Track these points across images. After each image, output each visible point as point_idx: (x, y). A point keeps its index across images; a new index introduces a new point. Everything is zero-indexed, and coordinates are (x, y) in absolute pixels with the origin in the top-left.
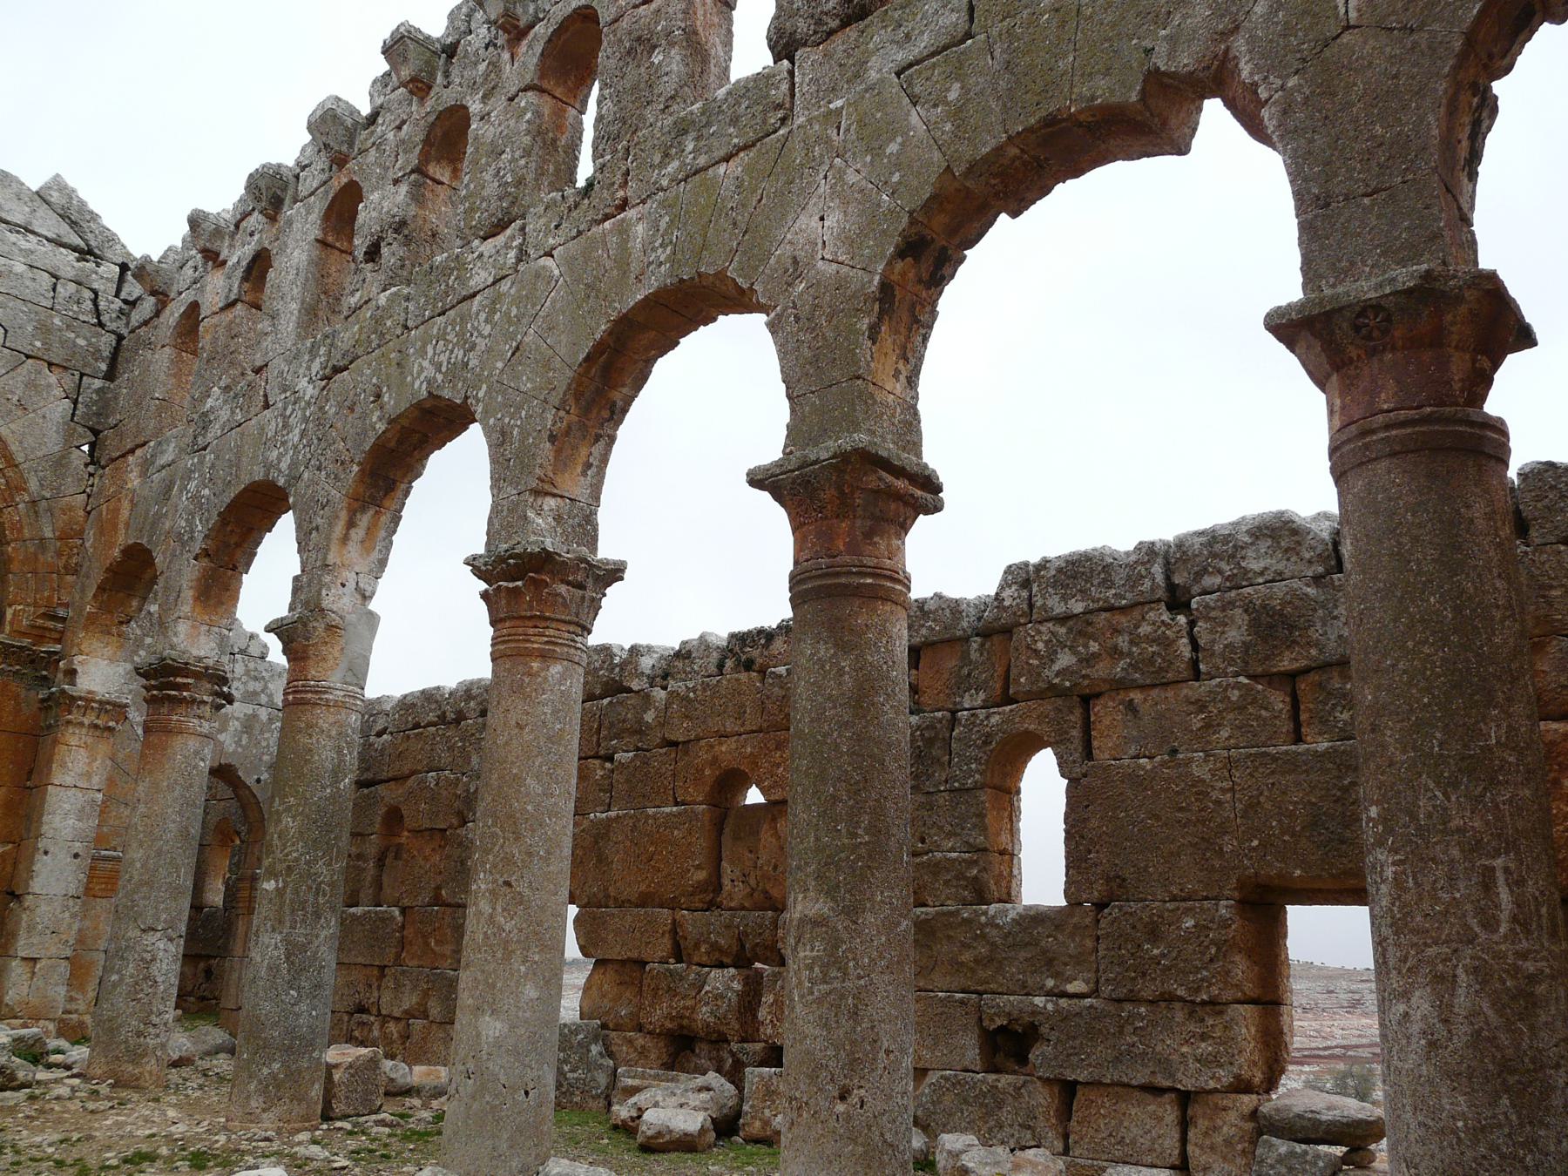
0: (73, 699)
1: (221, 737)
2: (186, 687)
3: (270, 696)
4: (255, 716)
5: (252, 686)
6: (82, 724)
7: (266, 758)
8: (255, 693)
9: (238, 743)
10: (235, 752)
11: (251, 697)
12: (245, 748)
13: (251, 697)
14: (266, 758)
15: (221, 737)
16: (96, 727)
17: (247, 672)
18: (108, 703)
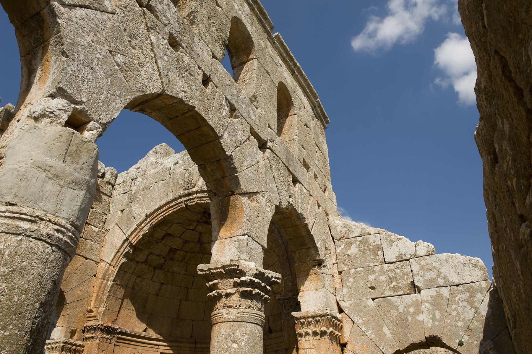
0: (297, 319)
1: (420, 318)
2: (214, 287)
3: (445, 278)
4: (439, 295)
5: (430, 275)
6: (307, 334)
7: (460, 324)
8: (433, 280)
9: (434, 318)
10: (433, 326)
11: (431, 284)
12: (439, 321)
13: (431, 284)
14: (460, 324)
15: (420, 318)
16: (315, 334)
17: (422, 268)
18: (317, 316)
